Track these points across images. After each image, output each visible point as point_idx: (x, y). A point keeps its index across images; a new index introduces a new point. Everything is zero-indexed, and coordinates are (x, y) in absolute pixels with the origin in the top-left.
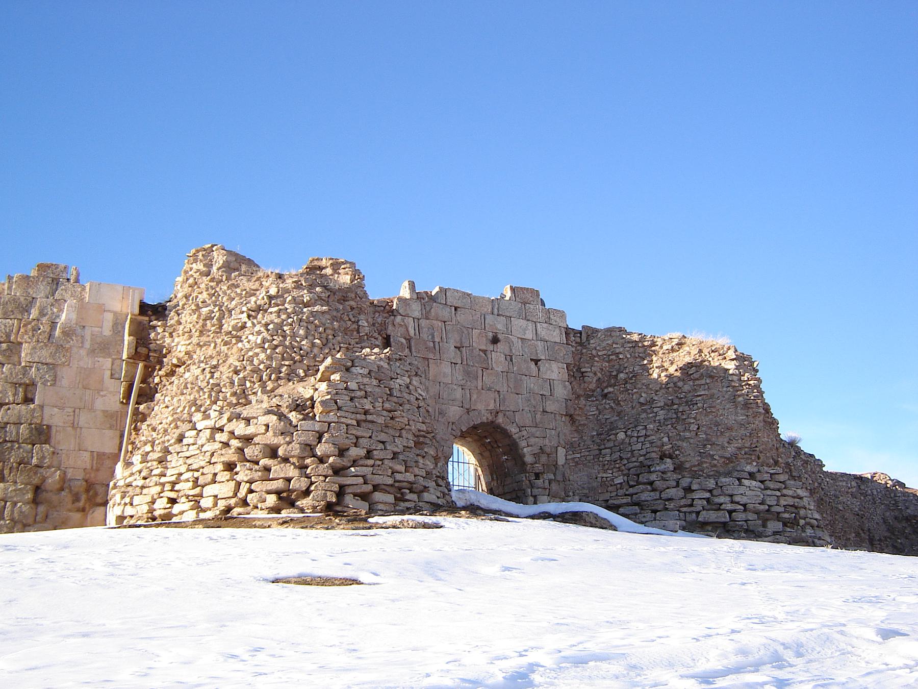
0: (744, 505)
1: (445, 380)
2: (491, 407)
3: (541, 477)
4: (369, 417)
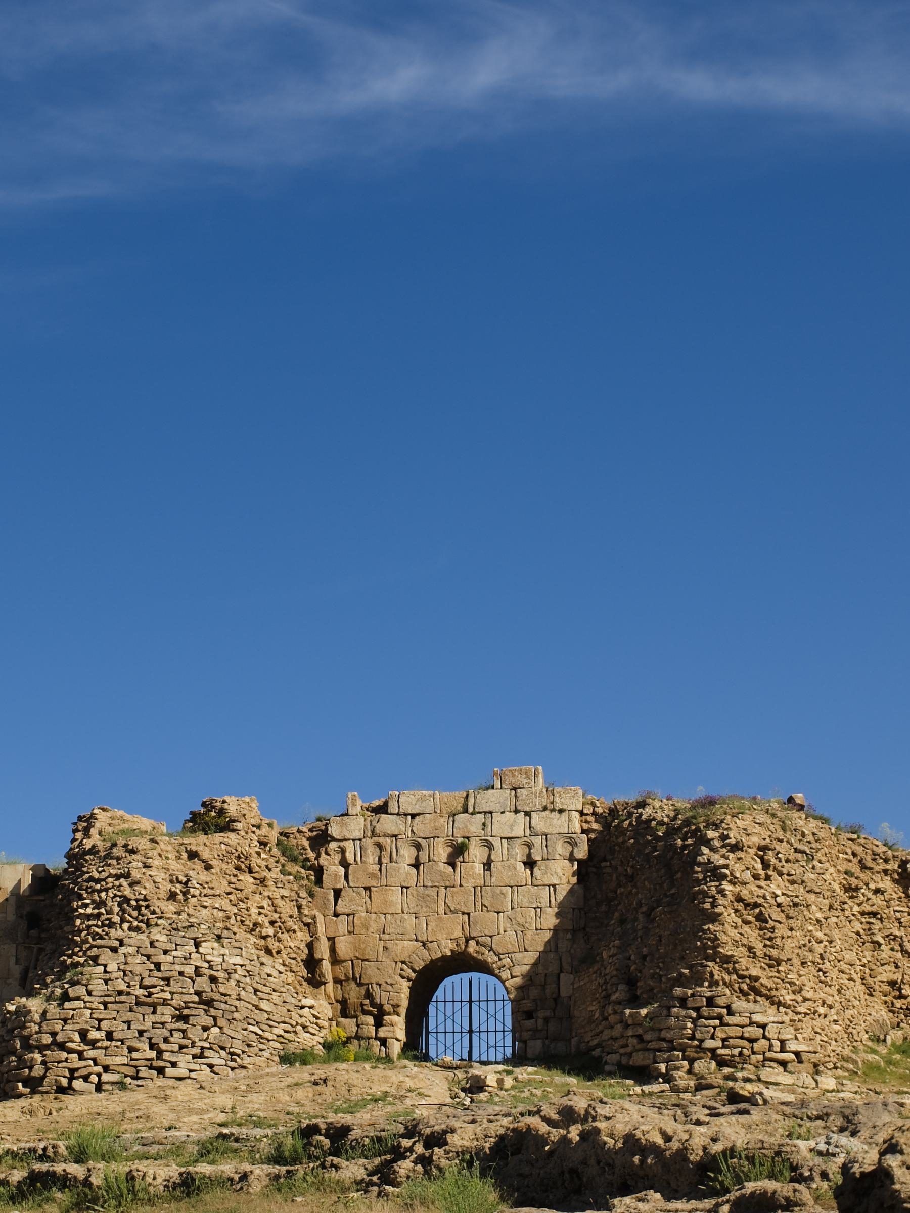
0: (671, 1041)
3: (534, 1016)
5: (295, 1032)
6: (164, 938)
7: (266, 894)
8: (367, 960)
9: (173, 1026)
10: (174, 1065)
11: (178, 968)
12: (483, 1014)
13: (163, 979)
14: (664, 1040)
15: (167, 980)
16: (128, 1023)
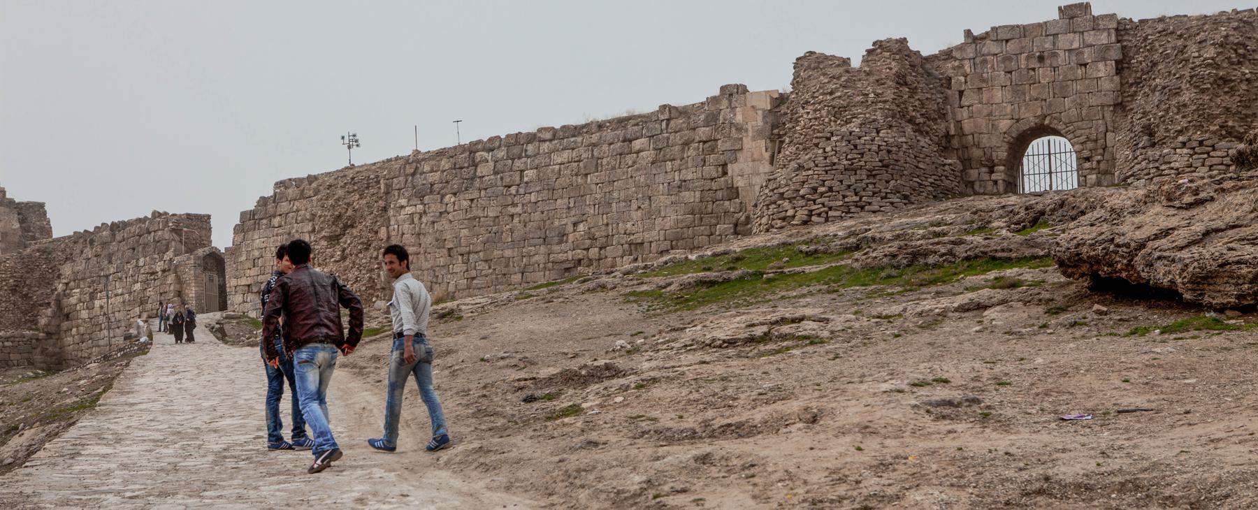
0: (1177, 169)
1: (997, 101)
2: (1039, 113)
4: (834, 167)
5: (941, 180)
6: (858, 130)
7: (917, 97)
8: (982, 133)
9: (868, 181)
10: (870, 204)
11: (868, 147)
12: (1058, 162)
13: (859, 154)
14: (1172, 168)
15: (862, 154)
16: (841, 181)
